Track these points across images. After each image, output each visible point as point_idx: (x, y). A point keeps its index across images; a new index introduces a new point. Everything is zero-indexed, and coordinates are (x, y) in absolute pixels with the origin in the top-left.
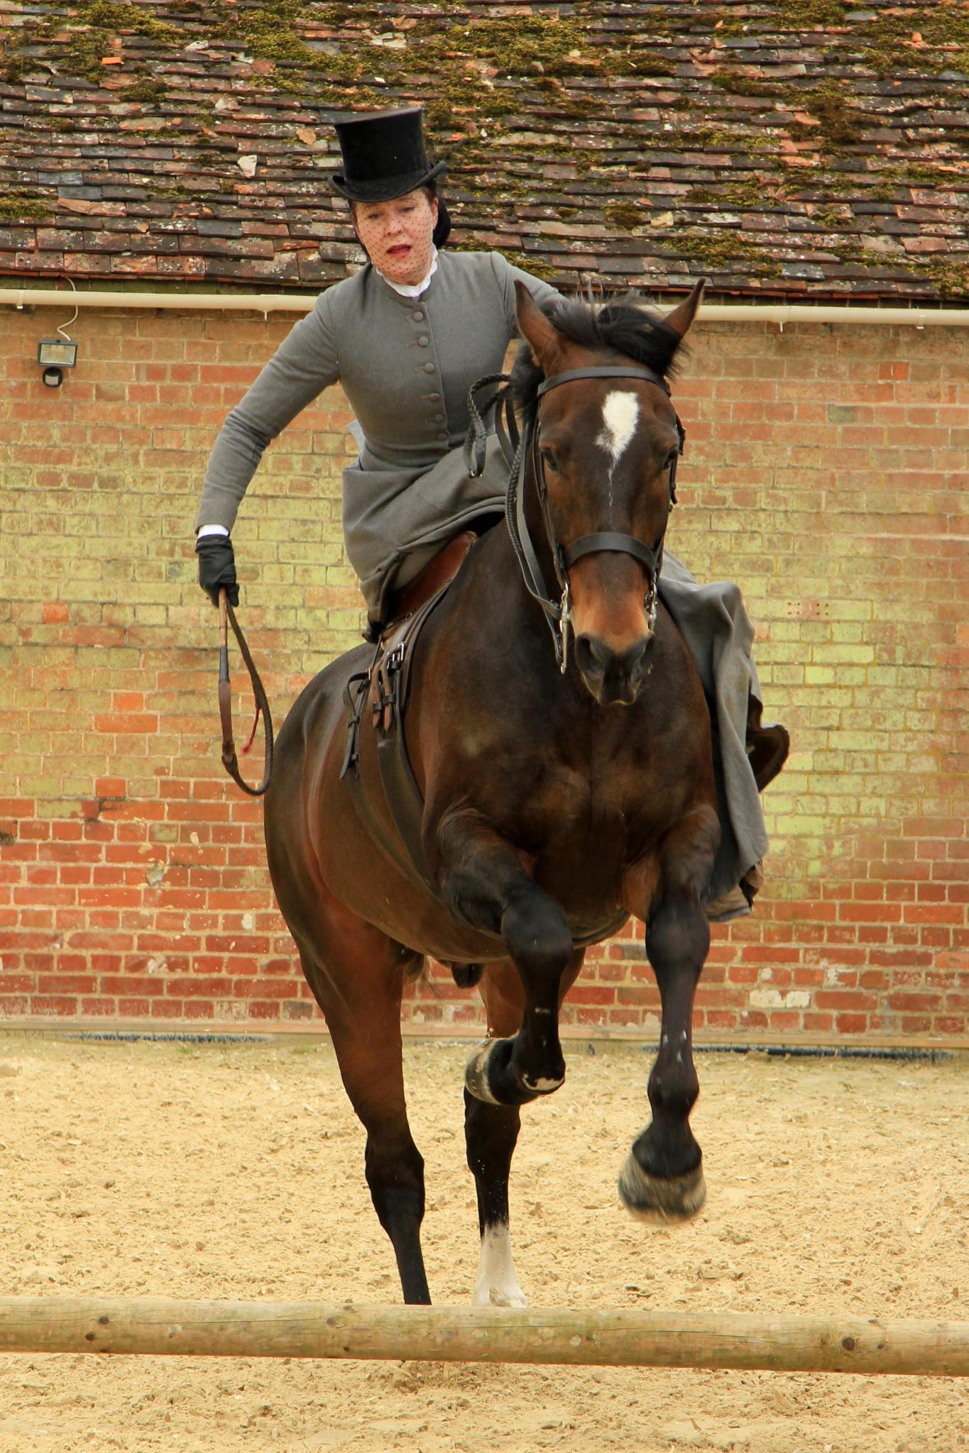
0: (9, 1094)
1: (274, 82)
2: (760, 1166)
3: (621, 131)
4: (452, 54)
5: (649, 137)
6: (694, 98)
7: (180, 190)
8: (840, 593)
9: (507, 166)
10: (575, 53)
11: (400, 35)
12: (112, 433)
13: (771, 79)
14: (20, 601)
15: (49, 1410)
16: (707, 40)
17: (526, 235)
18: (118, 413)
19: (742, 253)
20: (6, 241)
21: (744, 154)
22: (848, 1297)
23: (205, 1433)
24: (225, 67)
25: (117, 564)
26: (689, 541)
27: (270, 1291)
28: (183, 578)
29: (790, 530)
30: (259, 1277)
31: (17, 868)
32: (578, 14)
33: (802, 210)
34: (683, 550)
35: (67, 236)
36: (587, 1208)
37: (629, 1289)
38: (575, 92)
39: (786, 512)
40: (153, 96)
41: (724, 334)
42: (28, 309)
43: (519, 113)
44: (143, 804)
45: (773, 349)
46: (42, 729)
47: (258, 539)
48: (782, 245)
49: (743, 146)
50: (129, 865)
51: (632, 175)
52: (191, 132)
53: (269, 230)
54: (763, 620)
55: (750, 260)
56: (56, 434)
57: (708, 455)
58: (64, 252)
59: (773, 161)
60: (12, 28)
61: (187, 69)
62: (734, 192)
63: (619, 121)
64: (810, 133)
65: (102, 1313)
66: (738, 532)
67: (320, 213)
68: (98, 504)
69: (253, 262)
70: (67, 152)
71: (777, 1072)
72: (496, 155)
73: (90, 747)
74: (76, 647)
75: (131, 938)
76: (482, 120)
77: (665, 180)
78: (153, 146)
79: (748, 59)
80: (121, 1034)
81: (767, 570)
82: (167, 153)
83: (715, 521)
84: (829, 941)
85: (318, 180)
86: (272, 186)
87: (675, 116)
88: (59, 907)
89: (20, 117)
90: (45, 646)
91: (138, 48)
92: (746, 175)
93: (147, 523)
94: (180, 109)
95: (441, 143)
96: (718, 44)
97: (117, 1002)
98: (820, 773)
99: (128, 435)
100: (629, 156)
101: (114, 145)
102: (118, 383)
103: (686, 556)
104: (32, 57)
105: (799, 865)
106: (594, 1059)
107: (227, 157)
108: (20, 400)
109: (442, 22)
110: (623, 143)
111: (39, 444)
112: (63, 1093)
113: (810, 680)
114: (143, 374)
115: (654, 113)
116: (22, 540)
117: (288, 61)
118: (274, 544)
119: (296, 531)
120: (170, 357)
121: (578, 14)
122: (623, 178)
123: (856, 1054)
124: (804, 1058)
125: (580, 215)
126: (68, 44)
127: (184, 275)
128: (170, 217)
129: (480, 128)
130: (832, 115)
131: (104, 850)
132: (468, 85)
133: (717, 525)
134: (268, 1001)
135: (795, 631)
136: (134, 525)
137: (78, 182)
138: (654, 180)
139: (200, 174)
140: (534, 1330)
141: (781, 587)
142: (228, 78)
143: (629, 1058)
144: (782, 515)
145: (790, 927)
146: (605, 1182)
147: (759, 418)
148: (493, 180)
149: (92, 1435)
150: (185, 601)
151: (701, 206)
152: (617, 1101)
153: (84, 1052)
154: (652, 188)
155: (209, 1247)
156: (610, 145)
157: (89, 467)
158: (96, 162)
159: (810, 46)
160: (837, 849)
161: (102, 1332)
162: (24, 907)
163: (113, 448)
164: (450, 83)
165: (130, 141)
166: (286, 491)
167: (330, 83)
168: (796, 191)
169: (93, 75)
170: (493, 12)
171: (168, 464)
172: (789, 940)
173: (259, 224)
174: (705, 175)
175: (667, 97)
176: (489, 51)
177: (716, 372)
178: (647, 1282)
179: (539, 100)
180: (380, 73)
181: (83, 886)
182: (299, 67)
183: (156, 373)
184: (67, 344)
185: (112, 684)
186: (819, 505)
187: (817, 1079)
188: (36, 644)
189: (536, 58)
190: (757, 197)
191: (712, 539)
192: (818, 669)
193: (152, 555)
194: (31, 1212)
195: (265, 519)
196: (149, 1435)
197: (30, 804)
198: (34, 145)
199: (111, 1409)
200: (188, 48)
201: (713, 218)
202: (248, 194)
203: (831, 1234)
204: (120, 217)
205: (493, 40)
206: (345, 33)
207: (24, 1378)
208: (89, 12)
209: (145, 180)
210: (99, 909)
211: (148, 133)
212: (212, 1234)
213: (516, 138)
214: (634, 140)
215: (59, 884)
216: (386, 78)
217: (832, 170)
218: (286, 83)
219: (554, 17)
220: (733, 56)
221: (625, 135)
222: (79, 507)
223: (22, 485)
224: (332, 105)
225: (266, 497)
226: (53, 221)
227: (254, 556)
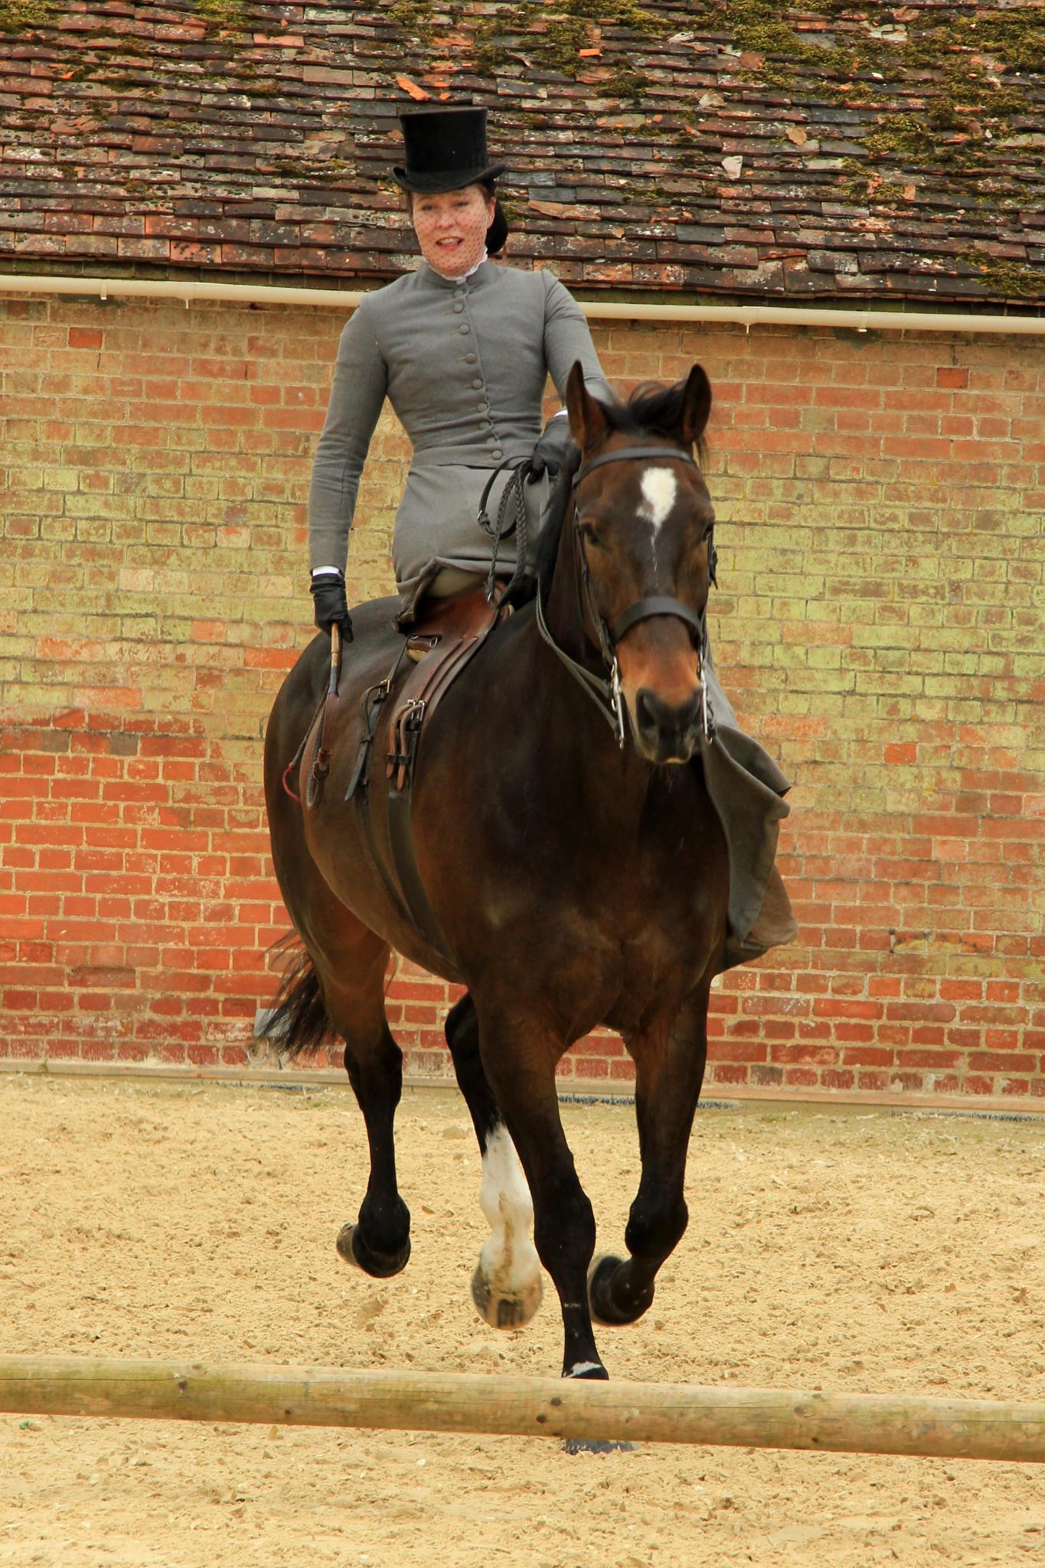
0: (459, 1157)
1: (761, 76)
4: (957, 48)
7: (660, 192)
11: (901, 27)
15: (497, 1495)
23: (662, 1525)
24: (711, 60)
27: (733, 1376)
30: (722, 1359)
40: (632, 91)
43: (1027, 113)
47: (734, 570)
52: (673, 130)
53: (752, 237)
58: (534, 258)
60: (484, 16)
61: (670, 63)
65: (554, 1394)
69: (736, 271)
70: (540, 151)
72: (1000, 157)
78: (631, 145)
80: (577, 1096)
82: (646, 153)
85: (808, 183)
86: (757, 190)
91: (618, 39)
94: (661, 105)
95: (940, 144)
97: (573, 1062)
101: (589, 144)
104: (505, 49)
109: (946, 14)
117: (779, 55)
118: (751, 575)
119: (775, 562)
120: (644, 372)
126: (544, 34)
127: (661, 284)
128: (648, 222)
129: (984, 128)
132: (973, 82)
134: (735, 1064)
137: (550, 183)
139: (681, 176)
140: (1018, 1426)
142: (714, 72)
148: (998, 185)
149: (542, 1524)
155: (668, 1326)
158: (570, 162)
161: (554, 1414)
165: (607, 139)
166: (765, 518)
173: (743, 230)
176: (996, 45)
180: (878, 68)
182: (791, 61)
195: (742, 548)
196: (603, 1526)
198: (504, 143)
199: (563, 1496)
200: (672, 40)
202: (732, 198)
204: (594, 221)
205: (1002, 33)
206: (842, 25)
207: (471, 1461)
209: (622, 182)
211: (626, 131)
212: (672, 1313)
216: (884, 74)
225: (743, 524)
226: (523, 224)
227: (728, 587)
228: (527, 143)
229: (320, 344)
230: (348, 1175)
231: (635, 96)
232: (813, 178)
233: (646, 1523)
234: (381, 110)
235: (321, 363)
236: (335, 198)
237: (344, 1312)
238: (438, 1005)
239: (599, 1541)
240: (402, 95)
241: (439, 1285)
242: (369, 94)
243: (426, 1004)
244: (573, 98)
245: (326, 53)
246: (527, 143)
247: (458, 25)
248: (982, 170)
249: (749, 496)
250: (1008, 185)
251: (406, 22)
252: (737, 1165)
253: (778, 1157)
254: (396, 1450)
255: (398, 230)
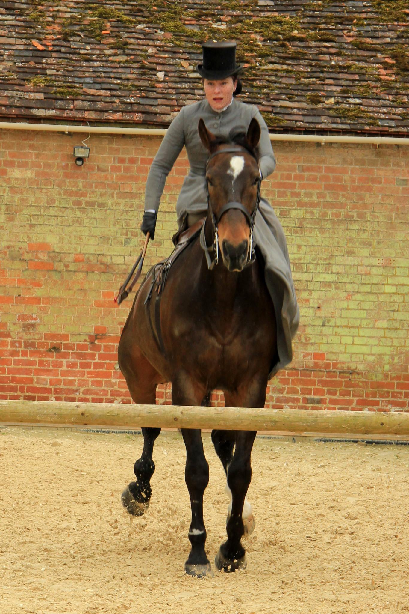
0: (58, 453)
1: (172, 42)
2: (362, 488)
3: (314, 64)
4: (245, 31)
5: (325, 67)
6: (344, 51)
7: (133, 86)
8: (399, 255)
9: (267, 78)
10: (296, 32)
12: (103, 185)
13: (376, 44)
14: (64, 253)
15: (72, 581)
16: (350, 27)
17: (273, 107)
18: (106, 176)
19: (362, 115)
20: (61, 105)
21: (364, 74)
22: (396, 542)
23: (135, 592)
24: (152, 35)
25: (105, 239)
26: (338, 233)
28: (131, 245)
29: (379, 229)
31: (62, 362)
32: (297, 16)
33: (387, 98)
34: (336, 236)
35: (87, 104)
36: (291, 504)
37: (308, 537)
38: (295, 48)
39: (378, 222)
40: (122, 47)
41: (354, 148)
42: (70, 134)
43: (272, 56)
44: (113, 337)
45: (374, 155)
46: (73, 305)
47: (162, 229)
48: (379, 112)
49: (364, 71)
50: (107, 361)
51: (318, 82)
53: (169, 102)
54: (368, 266)
55: (366, 118)
56: (80, 185)
57: (347, 198)
58: (85, 110)
59: (376, 78)
60: (66, 18)
61: (137, 36)
62: (359, 90)
63: (313, 60)
64: (391, 66)
66: (358, 230)
67: (190, 96)
68: (97, 214)
69: (162, 116)
70: (87, 69)
71: (370, 449)
72: (262, 73)
73: (92, 313)
74: (87, 272)
75: (108, 391)
76: (257, 59)
77: (331, 85)
78: (122, 67)
79: (366, 35)
80: (103, 430)
81: (370, 245)
82: (127, 70)
83: (349, 225)
84: (391, 397)
85: (189, 82)
86: (170, 85)
87: (336, 58)
88: (79, 378)
89: (68, 55)
90: (74, 272)
91: (117, 27)
92: (364, 83)
93: (117, 222)
94: (133, 52)
96: (354, 29)
98: (390, 329)
99: (110, 186)
100: (317, 74)
102: (106, 164)
103: (337, 239)
104: (73, 30)
105: (380, 366)
106: (295, 444)
107: (152, 73)
108: (66, 171)
109: (241, 18)
110: (314, 69)
111: (74, 189)
112: (79, 453)
113: (386, 291)
114: (116, 161)
115: (327, 57)
116: (66, 228)
117: (178, 33)
118: (169, 231)
120: (127, 154)
121: (297, 16)
122: (314, 83)
123: (402, 444)
124: (380, 445)
125: (296, 98)
126: (88, 25)
127: (134, 121)
128: (129, 97)
129: (256, 62)
130: (400, 59)
131: (97, 355)
133: (350, 227)
135: (381, 271)
136: (111, 223)
137: (91, 82)
138: (327, 85)
139: (141, 79)
141: (375, 252)
142: (153, 40)
143: (309, 444)
144: (376, 223)
145: (376, 392)
146: (299, 494)
147: (368, 183)
148: (261, 84)
150: (132, 254)
151: (346, 95)
152: (304, 461)
153: (88, 437)
154: (326, 88)
156: (309, 70)
157: (94, 199)
158: (99, 74)
159: (392, 30)
160: (396, 360)
162: (65, 378)
163: (104, 191)
164: (244, 43)
165: (113, 65)
167: (195, 43)
168: (385, 90)
169: (98, 38)
170: (262, 14)
171: (126, 198)
172: (376, 397)
173: (165, 100)
174: (348, 83)
175: (333, 51)
176: (260, 30)
177: (351, 164)
178: (315, 534)
179: (280, 51)
180: (216, 39)
181: (89, 370)
182: (183, 36)
183: (122, 161)
184: (85, 148)
185: (102, 287)
186: (392, 219)
187: (386, 454)
188: (71, 271)
189: (279, 34)
190: (369, 92)
191: (347, 232)
192: (390, 287)
193: (119, 235)
194: (66, 501)
196: (112, 592)
197: (67, 336)
198: (73, 66)
200: (137, 27)
201: (351, 101)
202: (161, 88)
203: (390, 516)
204: (108, 96)
205: (262, 26)
206: (202, 22)
208: (97, 12)
209: (119, 81)
210: (95, 379)
211: (120, 62)
213: (271, 66)
214: (319, 68)
215: (78, 369)
217: (400, 82)
218: (177, 42)
219: (287, 17)
220: (360, 34)
221: (315, 66)
222: (89, 215)
223: (66, 206)
224: (195, 52)
225: (165, 212)
226: (81, 97)
227: (160, 236)
228: (82, 67)
229: (3, 143)
230: (16, 461)
231: (124, 49)
232: (191, 80)
233: (129, 592)
234: (26, 54)
235: (4, 150)
236: (8, 87)
237: (14, 512)
238: (49, 395)
239: (111, 598)
240: (34, 48)
241: (50, 502)
242: (21, 47)
243: (45, 395)
244: (100, 50)
245: (5, 32)
246: (82, 67)
247: (56, 21)
248: (255, 78)
249: (168, 202)
250: (265, 84)
251: (36, 20)
252: (164, 456)
253: (179, 453)
254: (33, 565)
255: (33, 100)
